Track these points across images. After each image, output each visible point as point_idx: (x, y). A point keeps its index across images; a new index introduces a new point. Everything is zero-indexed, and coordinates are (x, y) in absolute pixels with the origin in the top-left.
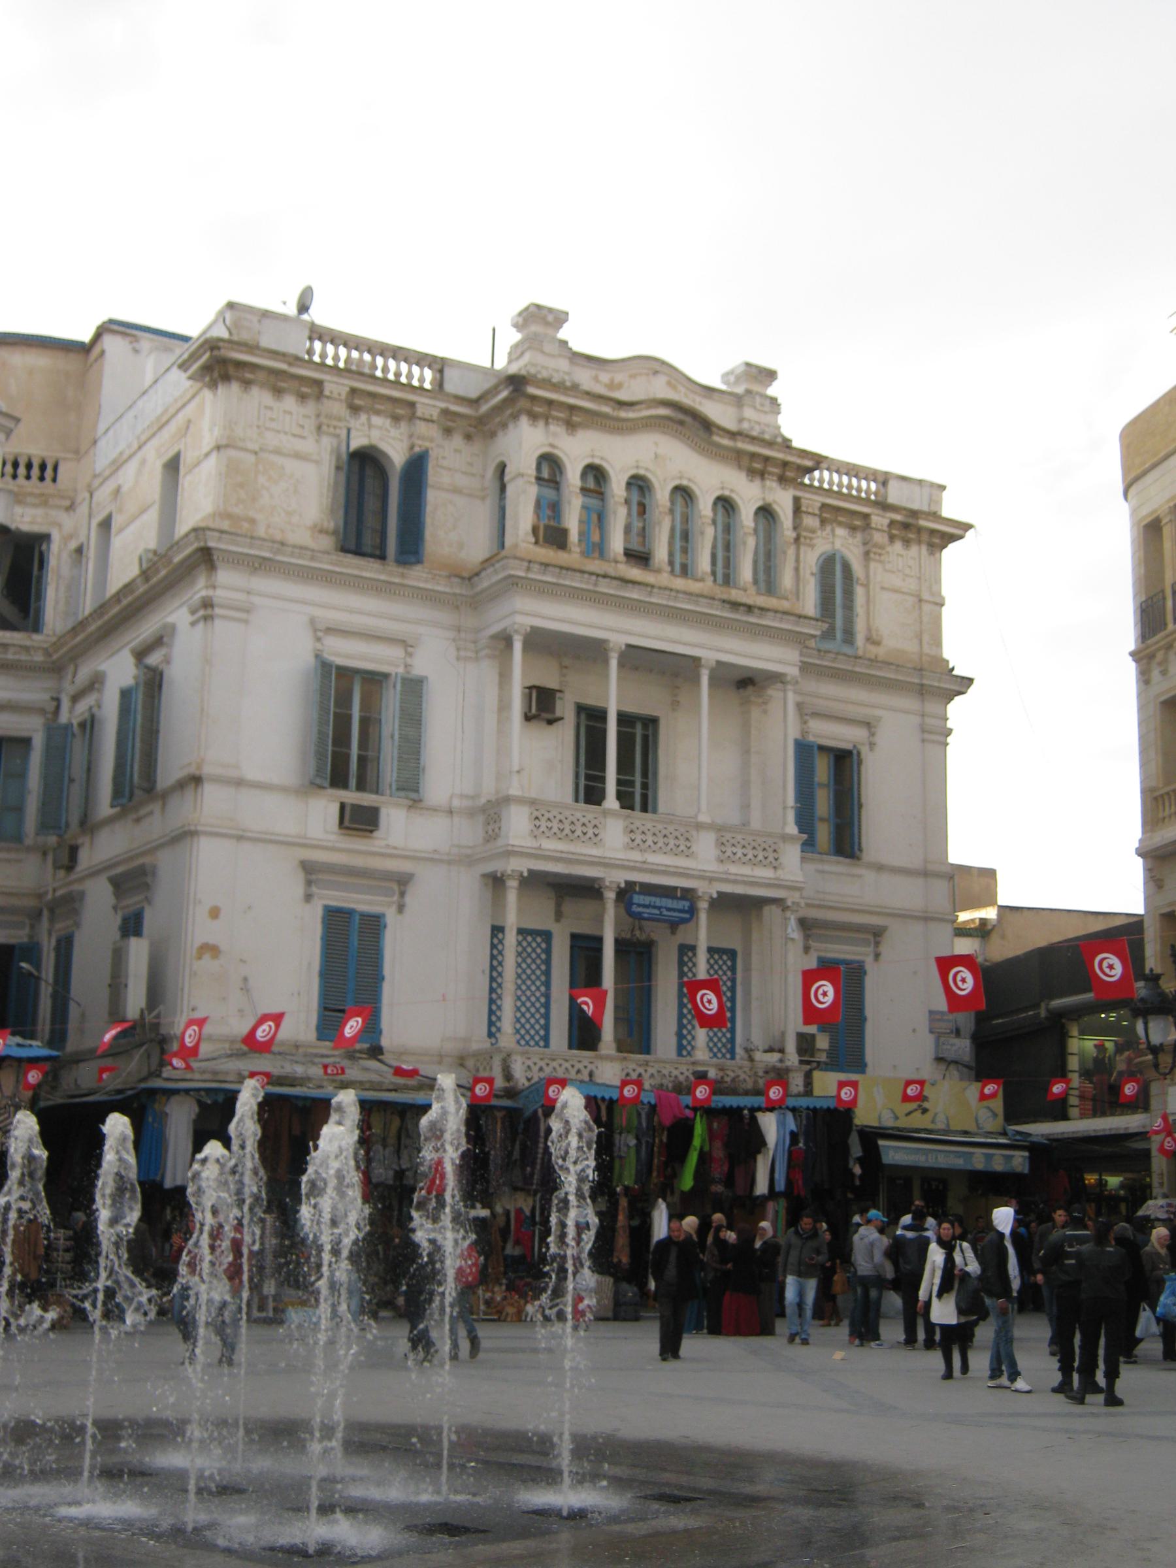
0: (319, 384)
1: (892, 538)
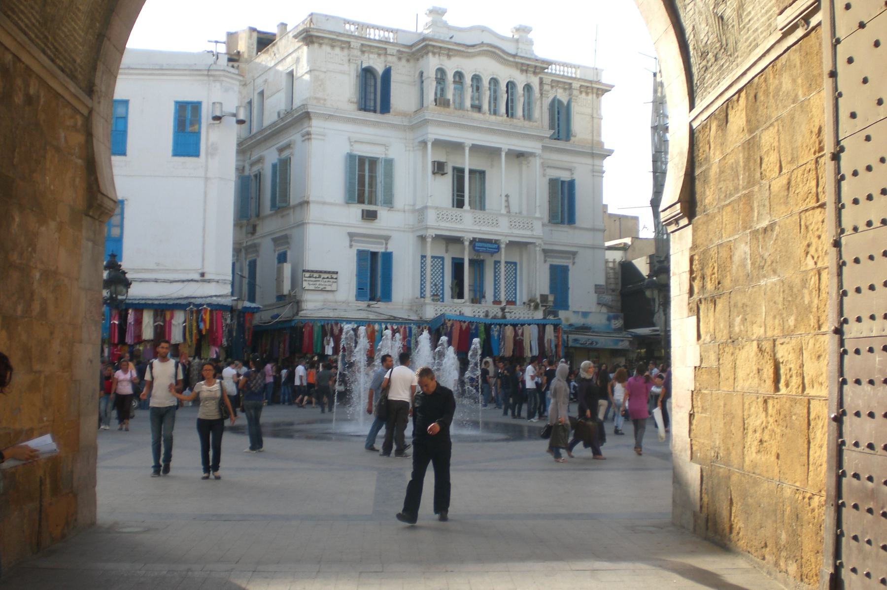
0: (349, 43)
1: (581, 92)
